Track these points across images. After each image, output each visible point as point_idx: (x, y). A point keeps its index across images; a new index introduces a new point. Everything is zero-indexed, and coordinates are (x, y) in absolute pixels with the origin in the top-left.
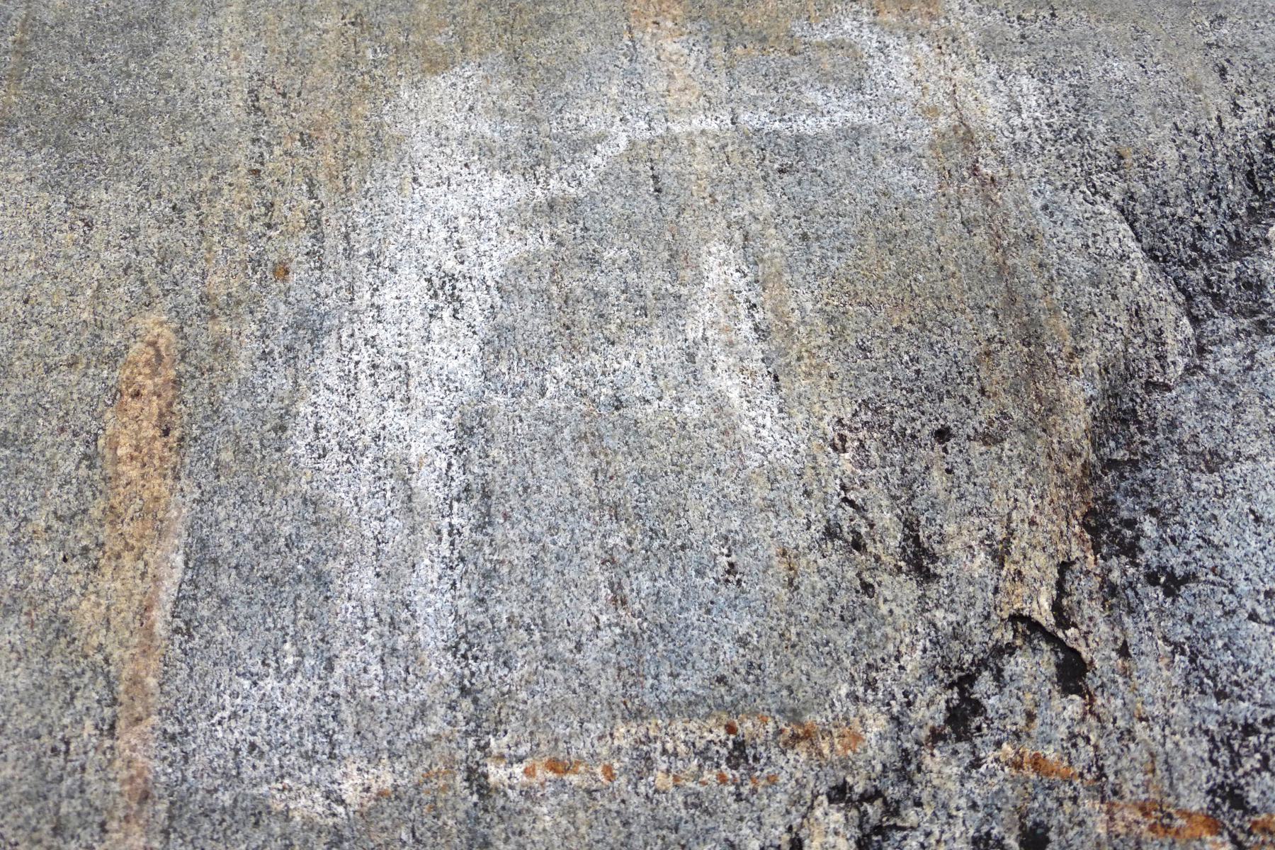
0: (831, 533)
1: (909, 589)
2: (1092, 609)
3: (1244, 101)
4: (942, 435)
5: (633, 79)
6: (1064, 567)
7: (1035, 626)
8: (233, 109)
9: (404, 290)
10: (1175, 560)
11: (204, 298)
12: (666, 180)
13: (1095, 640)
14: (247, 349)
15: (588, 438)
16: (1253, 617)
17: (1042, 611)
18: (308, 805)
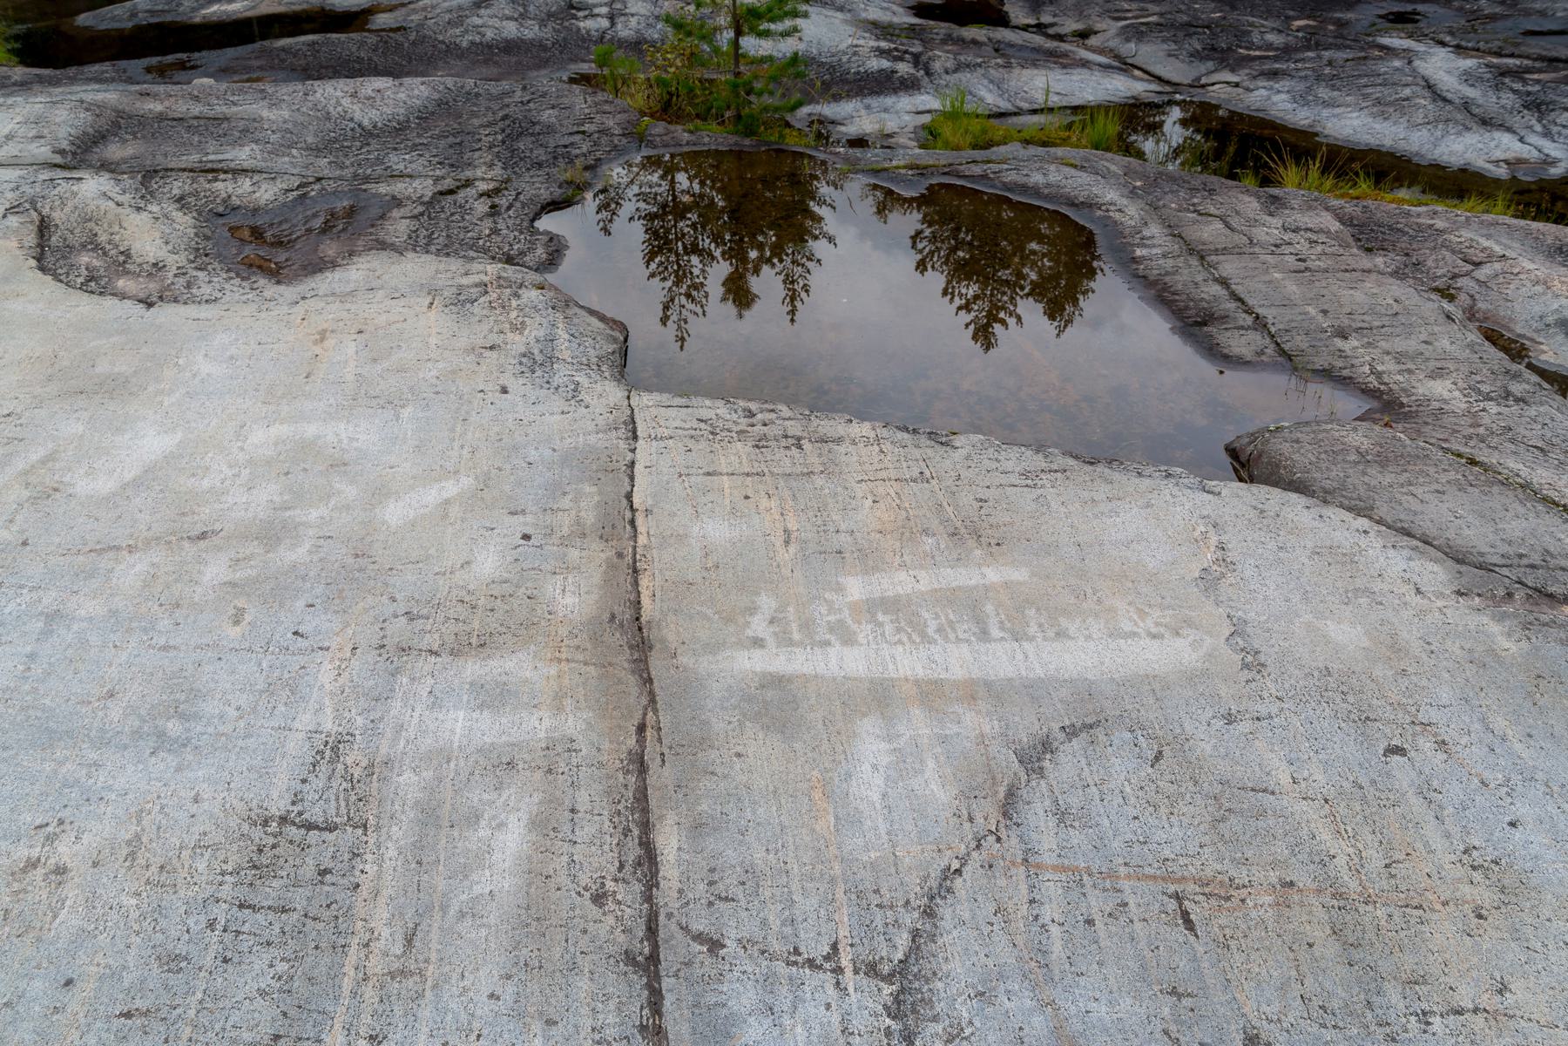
5: (909, 720)
8: (820, 726)
9: (866, 767)
13: (1004, 837)
15: (907, 797)
18: (865, 858)
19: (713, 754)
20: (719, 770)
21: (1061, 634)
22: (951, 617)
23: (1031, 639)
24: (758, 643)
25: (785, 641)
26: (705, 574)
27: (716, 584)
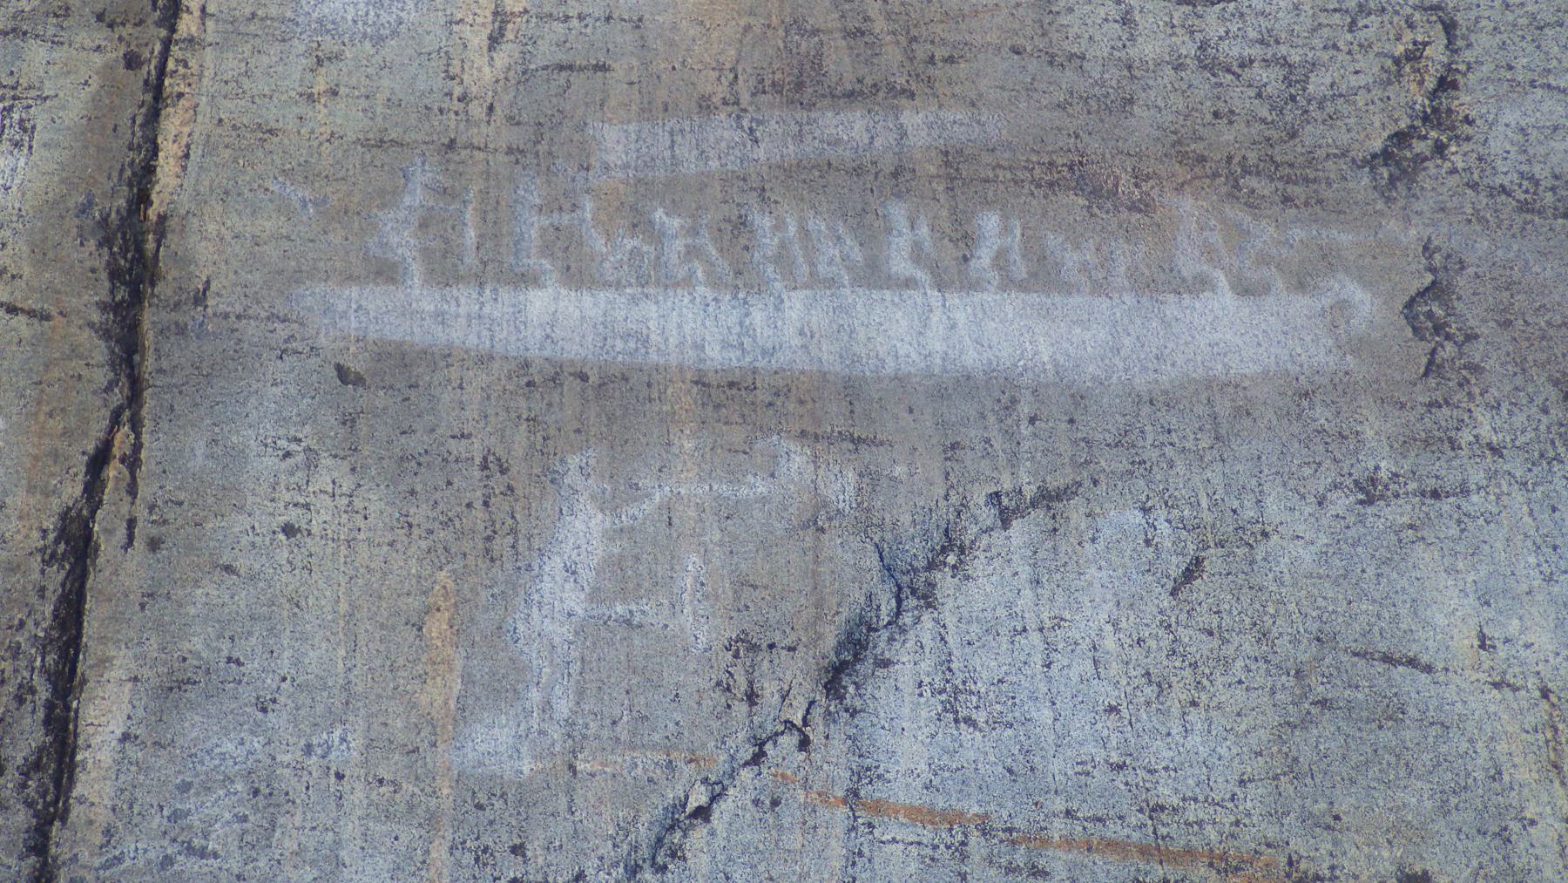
0: (718, 684)
1: (744, 707)
4: (772, 646)
6: (812, 703)
7: (794, 725)
9: (555, 565)
10: (858, 703)
12: (675, 520)
17: (798, 721)
19: (241, 522)
20: (242, 564)
23: (973, 286)
24: (386, 272)
25: (444, 270)
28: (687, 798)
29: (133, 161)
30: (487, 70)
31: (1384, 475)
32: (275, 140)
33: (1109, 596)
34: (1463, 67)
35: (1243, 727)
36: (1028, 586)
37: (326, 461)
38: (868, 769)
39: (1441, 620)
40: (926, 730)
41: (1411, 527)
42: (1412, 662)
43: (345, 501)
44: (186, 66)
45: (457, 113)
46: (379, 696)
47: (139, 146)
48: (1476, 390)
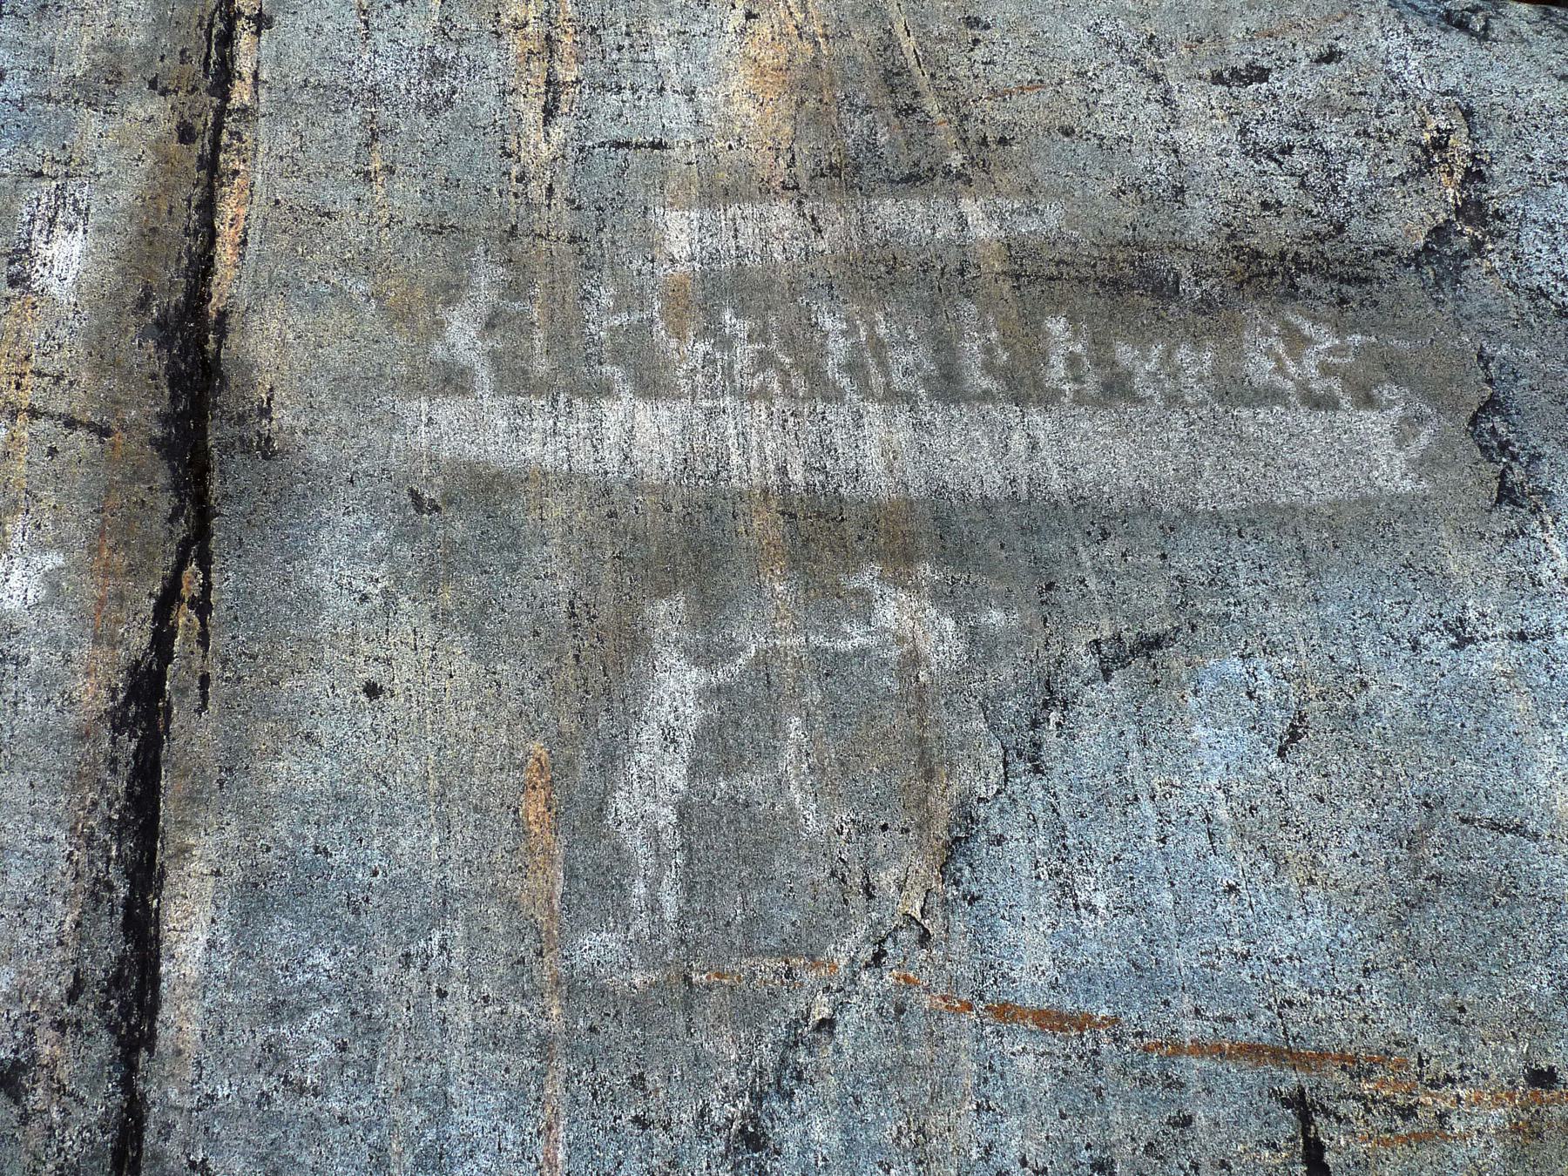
0: (833, 874)
2: (938, 911)
3: (1052, 640)
4: (884, 828)
9: (649, 734)
10: (974, 889)
11: (560, 734)
14: (583, 765)
16: (1003, 917)
21: (1117, 388)
22: (882, 330)
23: (1048, 399)
24: (454, 380)
26: (361, 190)
27: (385, 215)
28: (809, 1010)
29: (190, 247)
30: (543, 146)
31: (1472, 615)
32: (334, 224)
33: (1218, 759)
34: (1486, 158)
35: (1363, 907)
36: (1135, 747)
37: (405, 604)
38: (992, 967)
39: (1542, 782)
40: (1047, 919)
41: (1504, 674)
42: (1519, 830)
43: (428, 654)
44: (240, 140)
45: (516, 195)
46: (477, 894)
47: (196, 232)
48: (1549, 519)
